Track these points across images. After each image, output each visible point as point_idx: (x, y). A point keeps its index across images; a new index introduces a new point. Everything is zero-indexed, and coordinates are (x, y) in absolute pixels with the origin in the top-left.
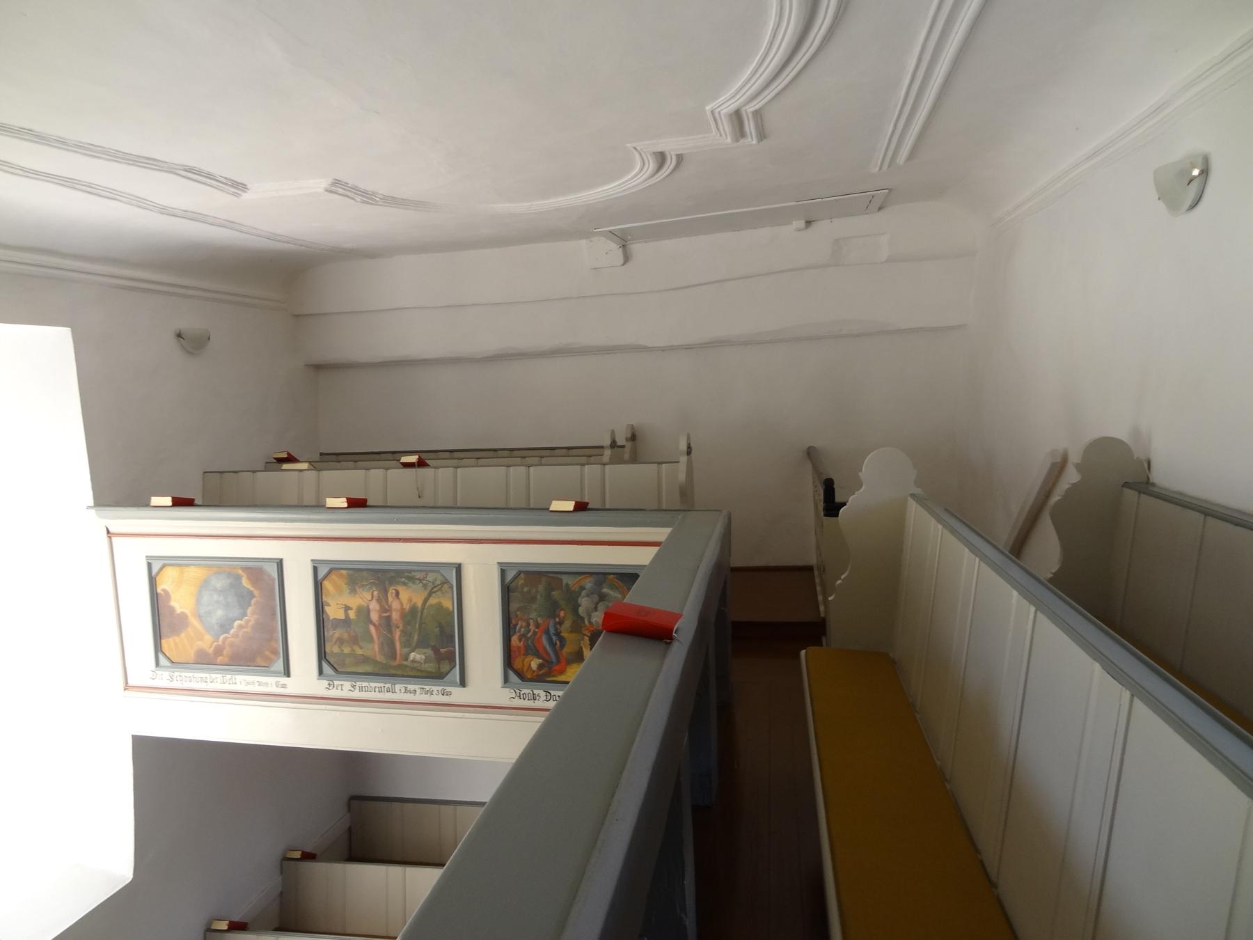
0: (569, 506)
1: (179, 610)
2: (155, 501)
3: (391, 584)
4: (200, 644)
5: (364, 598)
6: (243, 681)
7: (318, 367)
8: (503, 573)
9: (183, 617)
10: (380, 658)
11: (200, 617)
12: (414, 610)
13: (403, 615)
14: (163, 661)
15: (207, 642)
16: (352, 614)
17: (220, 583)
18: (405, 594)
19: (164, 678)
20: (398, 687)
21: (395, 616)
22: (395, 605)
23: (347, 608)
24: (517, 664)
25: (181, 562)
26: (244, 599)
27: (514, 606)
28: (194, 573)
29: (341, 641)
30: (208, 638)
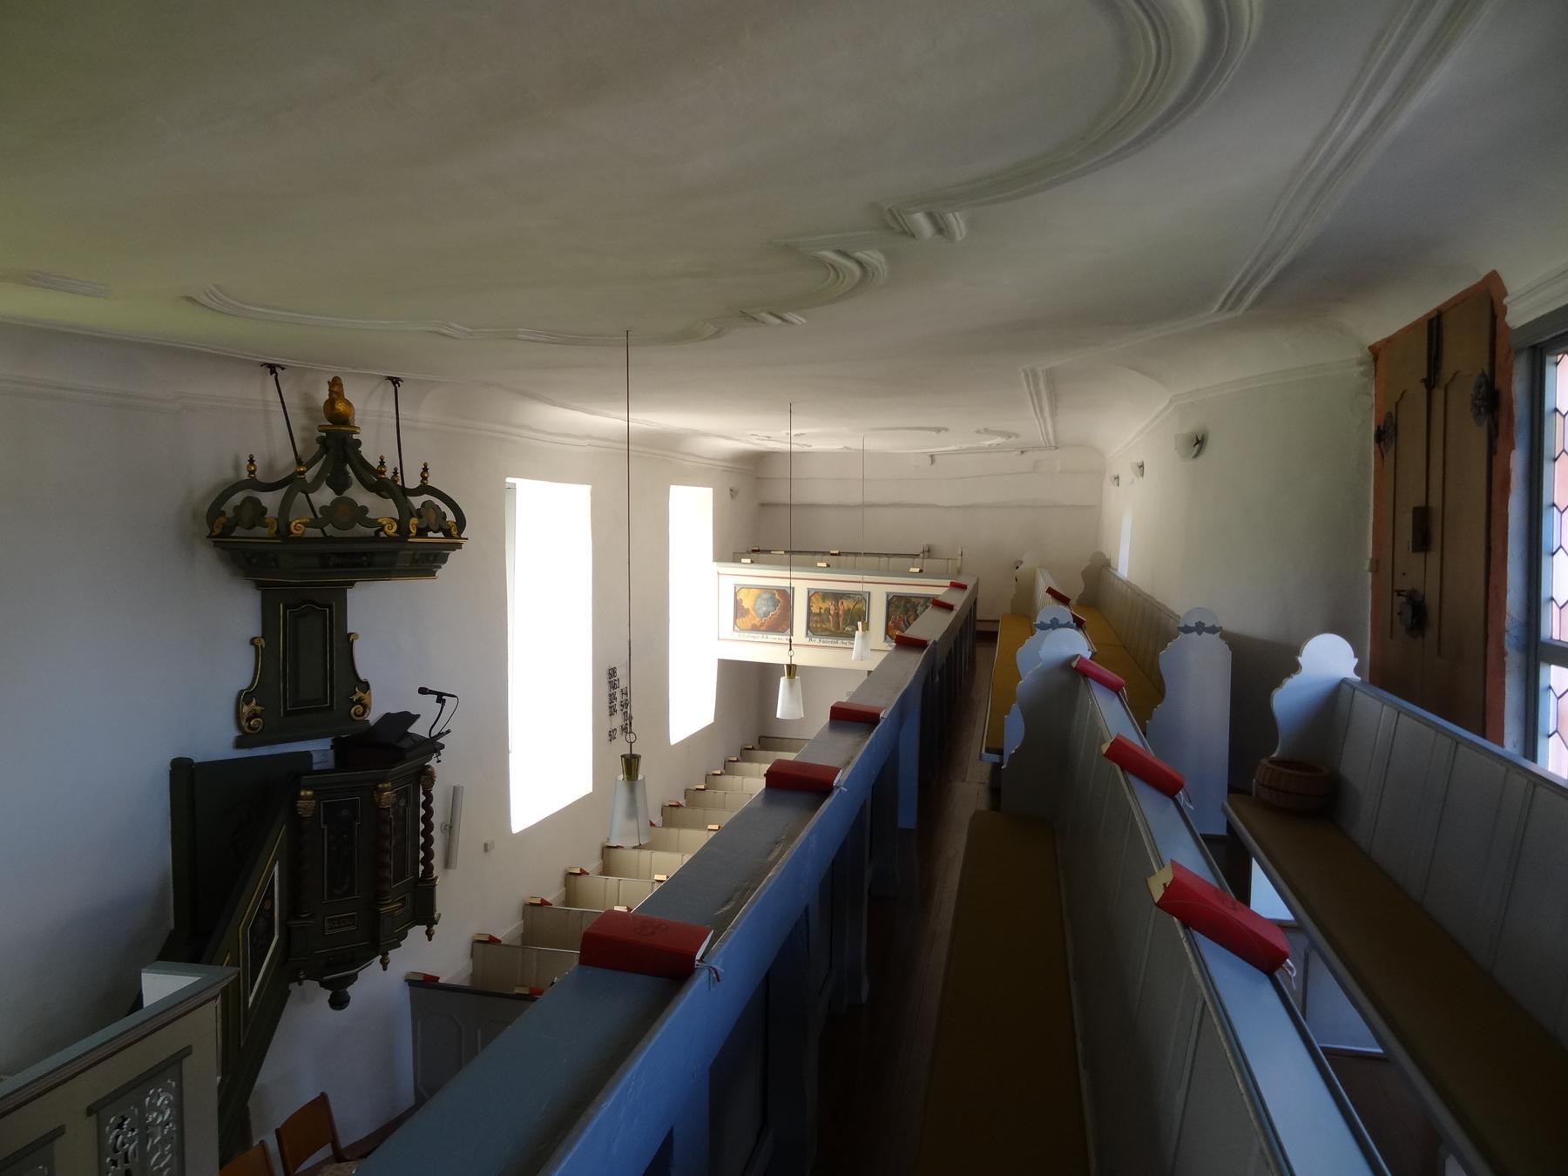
0: (918, 570)
1: (746, 607)
2: (743, 560)
3: (841, 598)
4: (754, 622)
5: (829, 604)
6: (772, 637)
7: (763, 505)
8: (888, 596)
9: (748, 609)
10: (833, 629)
11: (755, 610)
12: (849, 609)
13: (844, 611)
14: (736, 628)
15: (757, 621)
16: (822, 611)
17: (766, 596)
18: (845, 603)
19: (736, 636)
20: (839, 641)
21: (841, 612)
22: (841, 607)
23: (820, 608)
24: (890, 634)
25: (749, 587)
26: (776, 604)
27: (891, 609)
28: (754, 591)
29: (816, 622)
30: (758, 619)
